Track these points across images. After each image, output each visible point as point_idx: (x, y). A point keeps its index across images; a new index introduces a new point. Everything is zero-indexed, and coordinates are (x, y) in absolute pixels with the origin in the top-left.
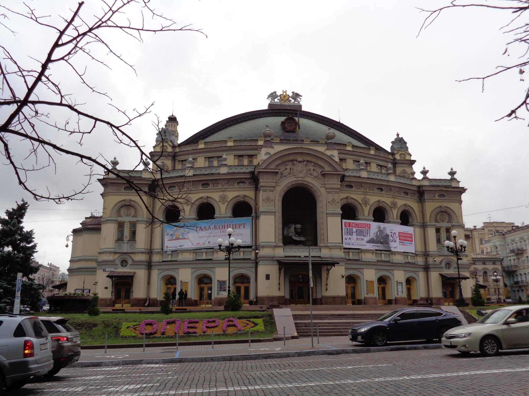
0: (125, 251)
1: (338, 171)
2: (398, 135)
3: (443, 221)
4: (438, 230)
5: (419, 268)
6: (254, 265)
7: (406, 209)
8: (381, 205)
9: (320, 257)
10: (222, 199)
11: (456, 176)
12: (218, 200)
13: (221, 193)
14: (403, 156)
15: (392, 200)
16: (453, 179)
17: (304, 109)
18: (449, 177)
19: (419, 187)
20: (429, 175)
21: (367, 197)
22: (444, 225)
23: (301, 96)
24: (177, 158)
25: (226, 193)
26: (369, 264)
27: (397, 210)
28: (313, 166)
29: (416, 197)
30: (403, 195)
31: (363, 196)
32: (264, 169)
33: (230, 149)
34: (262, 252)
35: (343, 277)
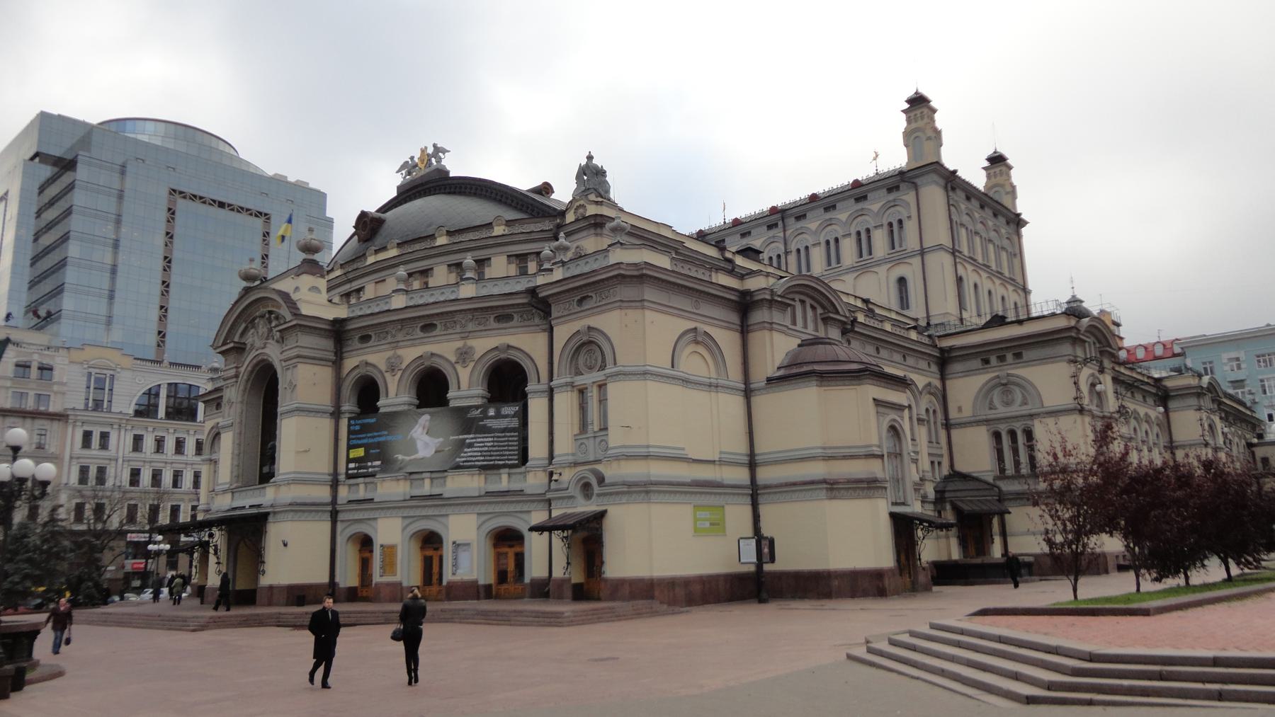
2: (590, 158)
3: (591, 368)
4: (582, 392)
5: (533, 501)
7: (503, 356)
8: (427, 363)
9: (259, 506)
14: (581, 210)
15: (460, 344)
19: (532, 292)
21: (400, 352)
22: (587, 379)
26: (389, 507)
27: (472, 364)
28: (277, 318)
29: (537, 321)
30: (496, 325)
31: (390, 353)
32: (224, 344)
35: (285, 545)
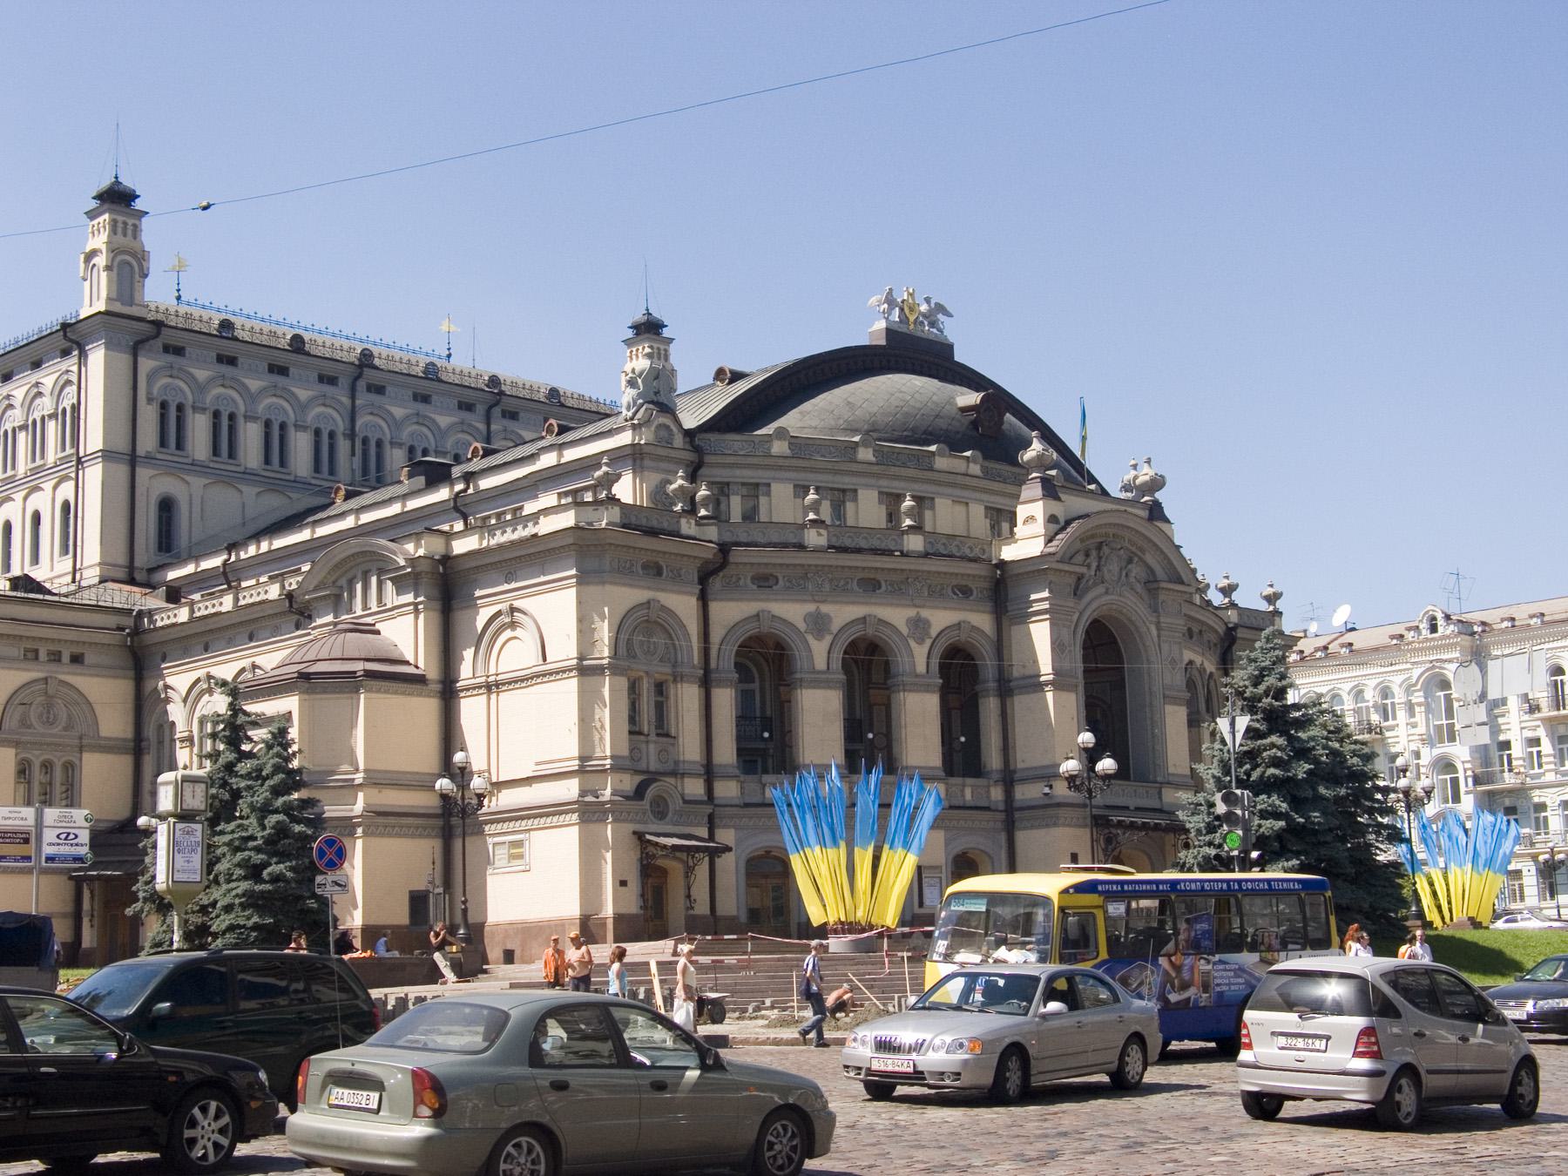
0: (652, 768)
1: (1182, 582)
6: (999, 825)
10: (919, 627)
11: (1280, 604)
12: (905, 631)
13: (911, 612)
16: (1277, 613)
17: (959, 357)
18: (1264, 606)
20: (1235, 596)
23: (950, 315)
24: (703, 471)
25: (925, 613)
33: (868, 473)
34: (1026, 793)
